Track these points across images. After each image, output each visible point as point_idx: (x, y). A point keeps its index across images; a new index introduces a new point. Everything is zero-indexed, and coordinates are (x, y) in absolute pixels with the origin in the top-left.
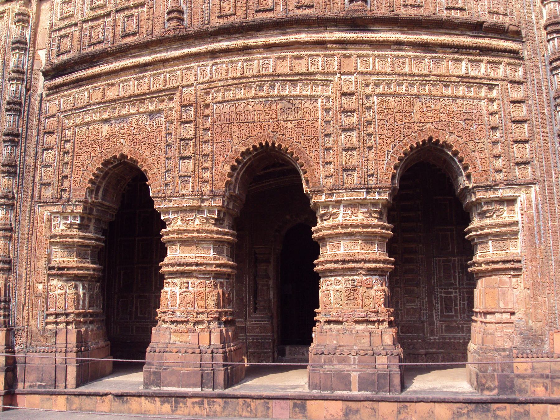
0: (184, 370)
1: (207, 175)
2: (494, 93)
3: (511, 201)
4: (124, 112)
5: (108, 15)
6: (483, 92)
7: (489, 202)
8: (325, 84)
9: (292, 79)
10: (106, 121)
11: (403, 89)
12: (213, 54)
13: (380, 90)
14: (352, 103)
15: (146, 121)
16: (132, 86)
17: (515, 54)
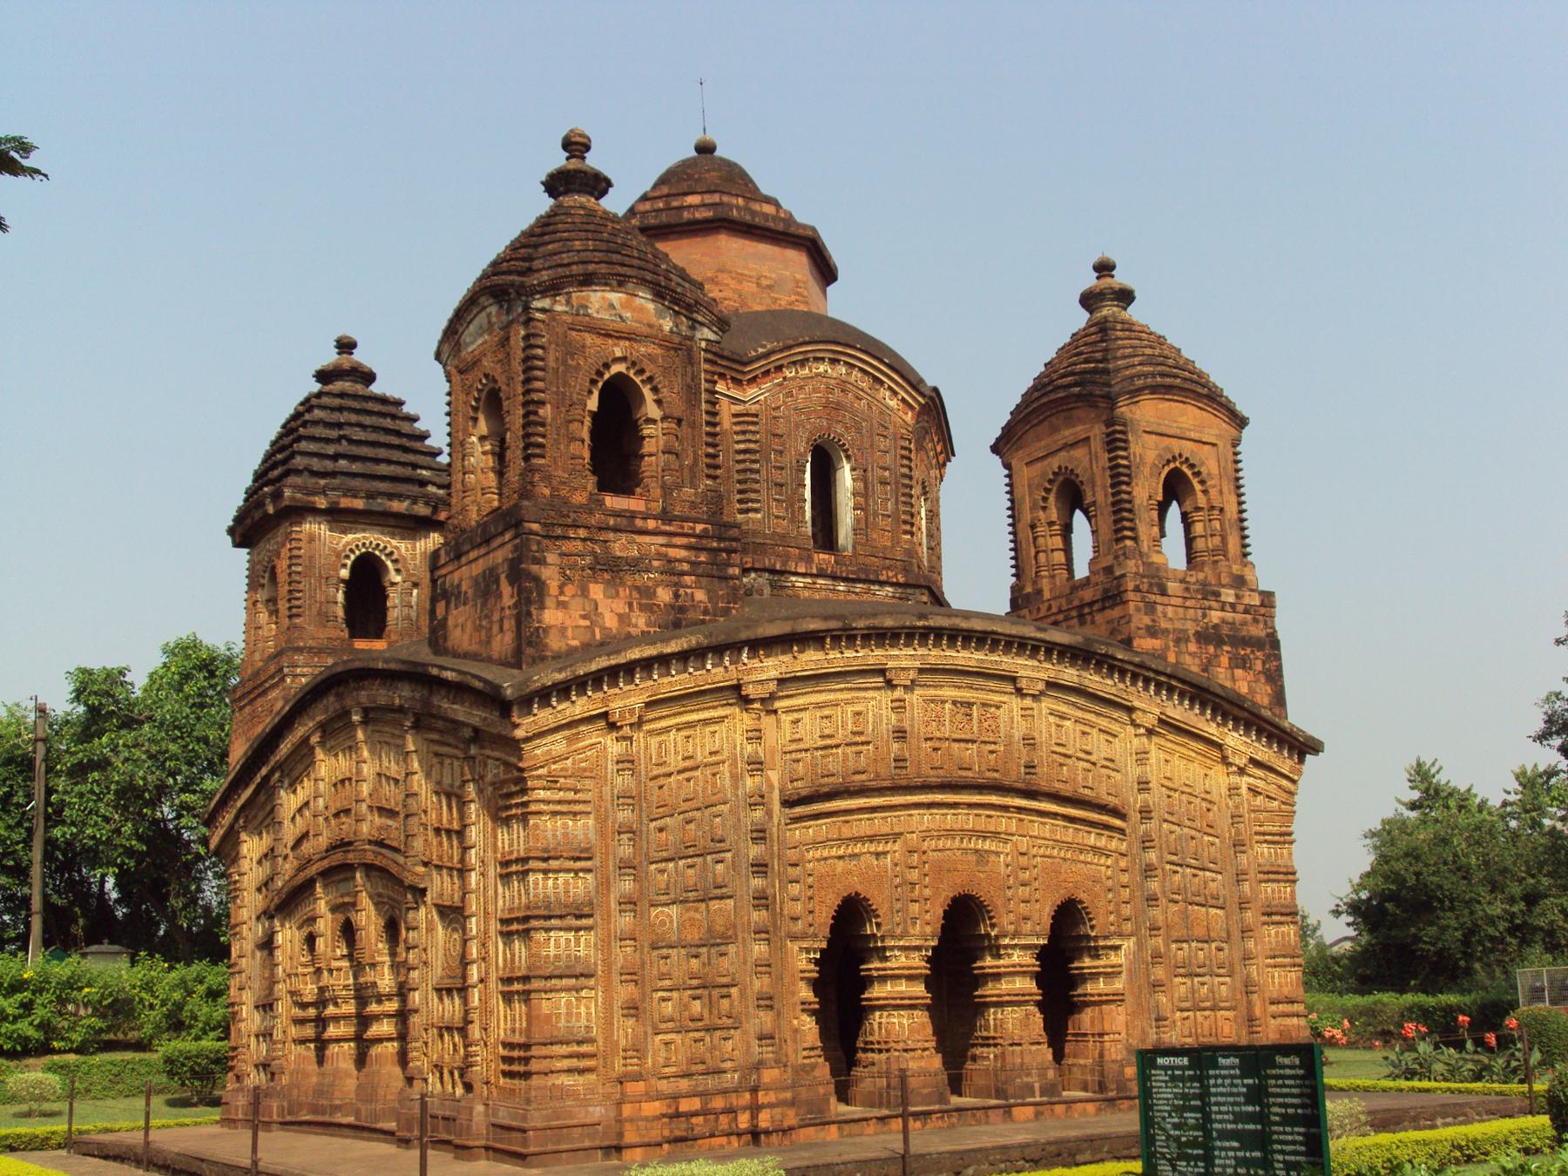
0: (925, 1091)
1: (928, 917)
2: (1109, 862)
3: (1117, 948)
4: (857, 851)
5: (837, 746)
6: (1103, 860)
7: (1104, 947)
8: (1006, 842)
9: (984, 835)
10: (840, 858)
11: (1055, 852)
12: (930, 805)
13: (1042, 851)
14: (1023, 860)
15: (873, 859)
16: (862, 825)
17: (1122, 831)
